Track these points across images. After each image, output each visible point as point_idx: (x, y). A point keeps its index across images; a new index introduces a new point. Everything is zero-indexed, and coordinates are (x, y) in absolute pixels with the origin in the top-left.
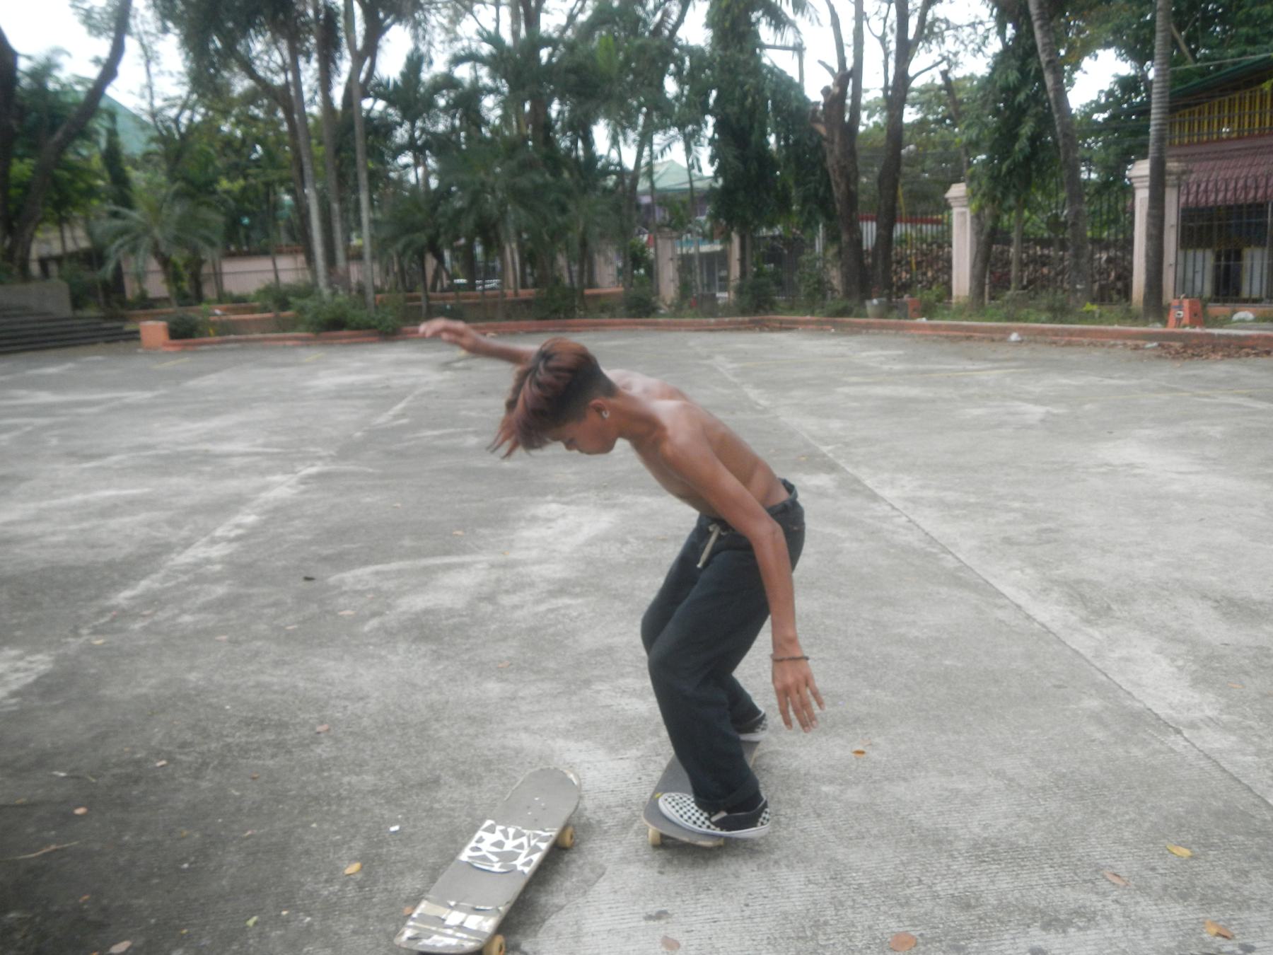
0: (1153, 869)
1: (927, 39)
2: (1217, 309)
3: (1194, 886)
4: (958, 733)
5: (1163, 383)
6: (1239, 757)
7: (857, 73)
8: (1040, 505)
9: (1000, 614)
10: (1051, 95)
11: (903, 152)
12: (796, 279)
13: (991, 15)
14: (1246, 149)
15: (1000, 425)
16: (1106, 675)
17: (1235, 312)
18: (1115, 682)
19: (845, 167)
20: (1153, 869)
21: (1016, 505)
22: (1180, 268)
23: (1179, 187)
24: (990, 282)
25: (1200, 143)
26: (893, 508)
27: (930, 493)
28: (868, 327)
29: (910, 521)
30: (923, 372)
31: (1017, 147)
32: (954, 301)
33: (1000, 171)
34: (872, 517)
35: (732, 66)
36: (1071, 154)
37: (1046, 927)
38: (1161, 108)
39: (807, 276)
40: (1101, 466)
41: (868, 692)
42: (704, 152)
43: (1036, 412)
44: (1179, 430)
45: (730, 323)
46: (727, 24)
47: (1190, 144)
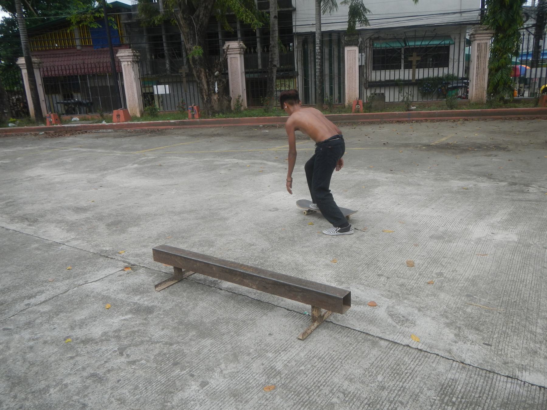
2: (65, 117)
5: (48, 147)
6: (82, 245)
8: (5, 195)
14: (65, 54)
17: (72, 118)
22: (47, 102)
23: (40, 69)
25: (46, 50)
40: (27, 178)
44: (56, 161)
47: (42, 51)
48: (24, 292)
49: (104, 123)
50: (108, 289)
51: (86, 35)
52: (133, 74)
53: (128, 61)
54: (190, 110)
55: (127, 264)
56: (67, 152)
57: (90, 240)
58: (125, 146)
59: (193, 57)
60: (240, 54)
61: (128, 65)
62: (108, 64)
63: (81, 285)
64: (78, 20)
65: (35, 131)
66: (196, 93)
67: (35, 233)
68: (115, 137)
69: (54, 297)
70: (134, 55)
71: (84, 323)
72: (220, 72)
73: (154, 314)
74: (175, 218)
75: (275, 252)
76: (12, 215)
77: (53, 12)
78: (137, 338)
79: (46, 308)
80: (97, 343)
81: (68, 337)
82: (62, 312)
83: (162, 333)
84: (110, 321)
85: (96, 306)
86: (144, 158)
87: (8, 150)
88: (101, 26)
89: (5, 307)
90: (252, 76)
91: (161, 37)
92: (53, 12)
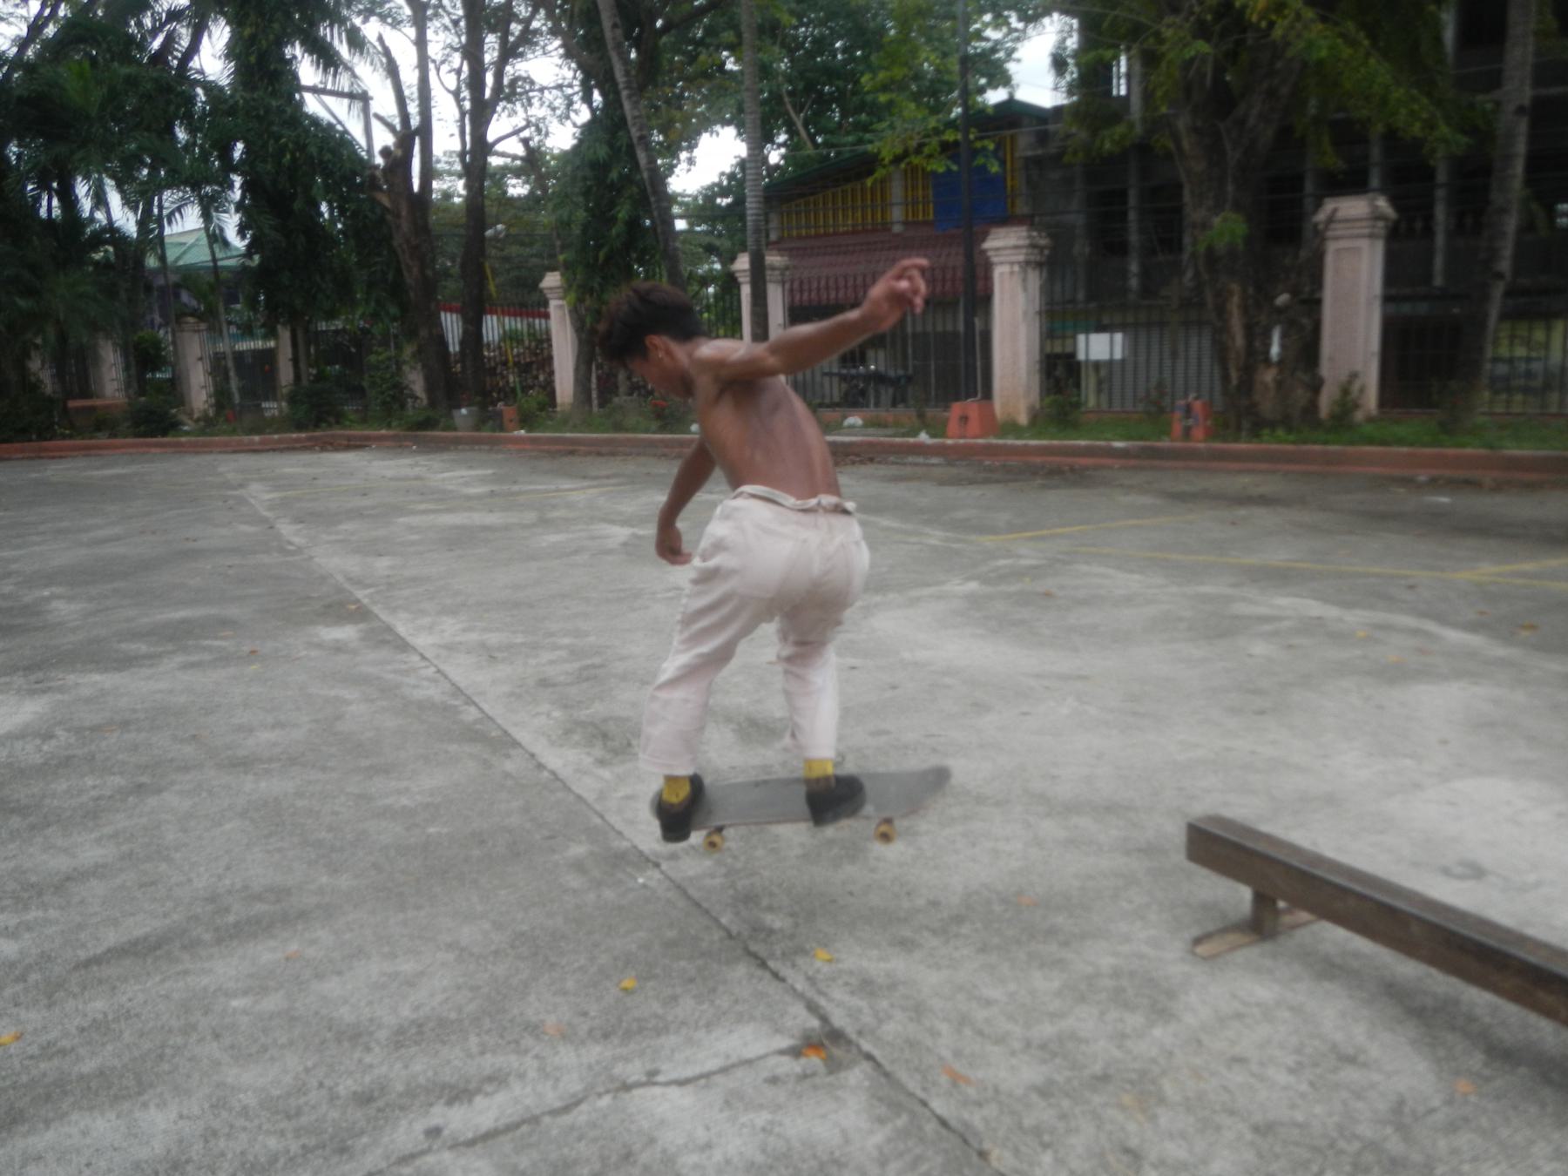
0: (585, 1014)
1: (511, 97)
4: (418, 908)
7: (425, 131)
8: (592, 639)
9: (509, 766)
10: (646, 175)
11: (489, 233)
12: (365, 384)
13: (575, 78)
15: (576, 552)
16: (602, 817)
17: (845, 417)
18: (609, 824)
20: (585, 1014)
21: (566, 641)
23: (783, 283)
25: (817, 236)
26: (423, 658)
27: (474, 637)
28: (457, 442)
29: (439, 671)
31: (614, 231)
32: (558, 409)
33: (596, 259)
34: (395, 672)
35: (262, 113)
36: (671, 244)
38: (755, 196)
39: (378, 381)
40: (669, 590)
41: (324, 879)
42: (230, 223)
45: (280, 441)
46: (253, 59)
47: (808, 237)
48: (454, 1061)
49: (923, 437)
50: (708, 1146)
51: (920, 192)
52: (1021, 298)
53: (1012, 263)
54: (1178, 415)
58: (960, 515)
59: (1210, 250)
60: (1371, 236)
61: (1012, 273)
62: (959, 274)
64: (899, 150)
66: (1206, 361)
67: (602, 796)
68: (942, 483)
69: (524, 1122)
70: (1033, 246)
72: (1295, 293)
74: (1049, 828)
75: (1464, 1139)
77: (850, 139)
86: (1002, 562)
88: (955, 168)
90: (1406, 308)
91: (1122, 195)
92: (850, 139)
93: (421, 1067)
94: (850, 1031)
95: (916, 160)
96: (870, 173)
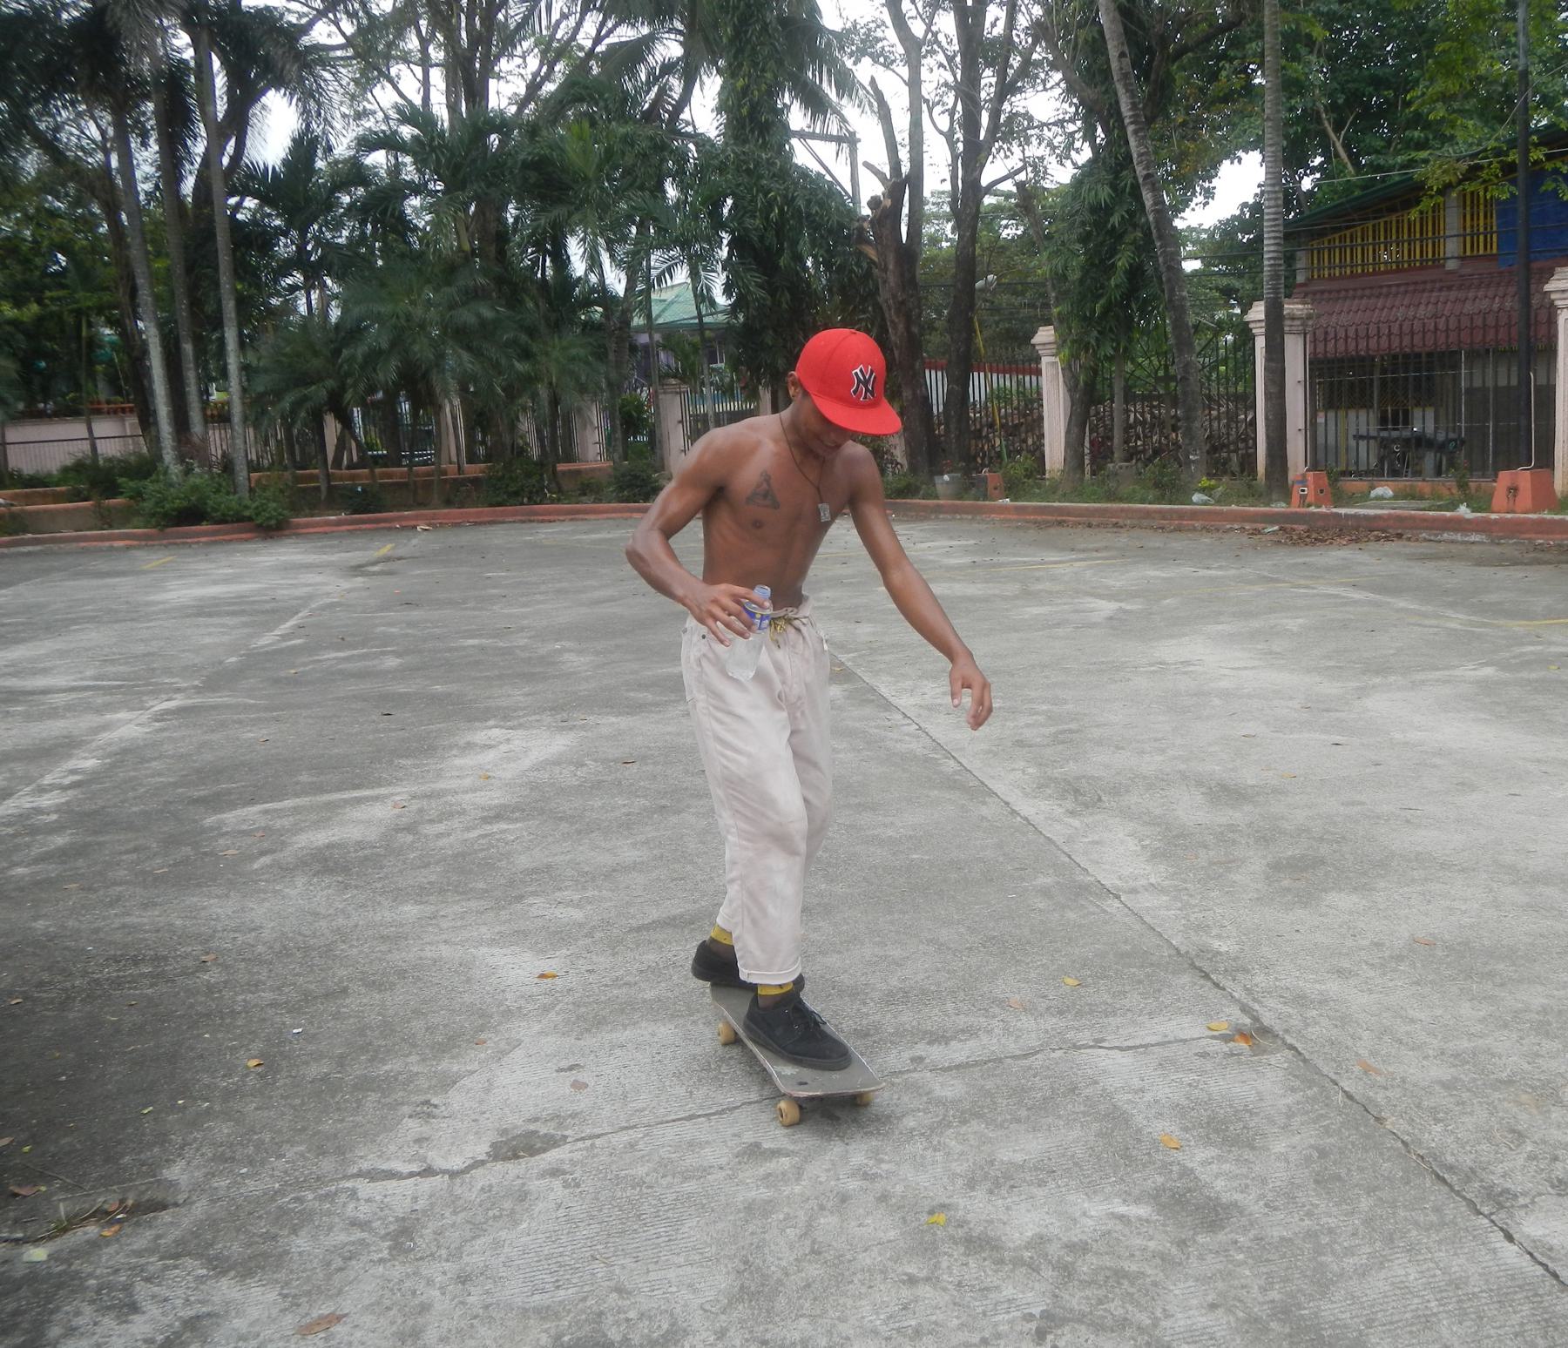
2: (1353, 485)
3: (1074, 1004)
4: (905, 913)
5: (1266, 574)
6: (1163, 912)
8: (1070, 707)
9: (984, 811)
10: (1151, 218)
11: (979, 284)
15: (1058, 625)
16: (1069, 857)
19: (903, 303)
21: (1044, 707)
23: (1305, 334)
24: (1091, 452)
25: (1353, 276)
28: (938, 510)
29: (920, 728)
30: (994, 566)
31: (1113, 282)
32: (1047, 476)
37: (930, 1043)
40: (1151, 665)
43: (1107, 607)
44: (1256, 624)
47: (1342, 277)
51: (1482, 224)
55: (1248, 1021)
56: (1306, 595)
57: (1193, 902)
58: (1493, 597)
63: (1080, 1048)
65: (1256, 522)
67: (1070, 840)
68: (1480, 562)
69: (990, 1061)
71: (1008, 1177)
73: (1221, 1237)
76: (1049, 773)
78: (1117, 1302)
79: (950, 1089)
80: (1001, 1262)
81: (944, 1207)
82: (978, 1116)
83: (1202, 1320)
84: (1079, 1202)
85: (1076, 1133)
87: (1157, 573)
89: (867, 1048)
93: (907, 1018)
94: (1278, 1028)
95: (1470, 187)
96: (1418, 202)
